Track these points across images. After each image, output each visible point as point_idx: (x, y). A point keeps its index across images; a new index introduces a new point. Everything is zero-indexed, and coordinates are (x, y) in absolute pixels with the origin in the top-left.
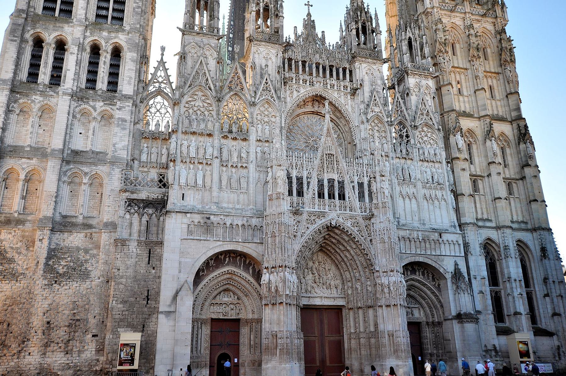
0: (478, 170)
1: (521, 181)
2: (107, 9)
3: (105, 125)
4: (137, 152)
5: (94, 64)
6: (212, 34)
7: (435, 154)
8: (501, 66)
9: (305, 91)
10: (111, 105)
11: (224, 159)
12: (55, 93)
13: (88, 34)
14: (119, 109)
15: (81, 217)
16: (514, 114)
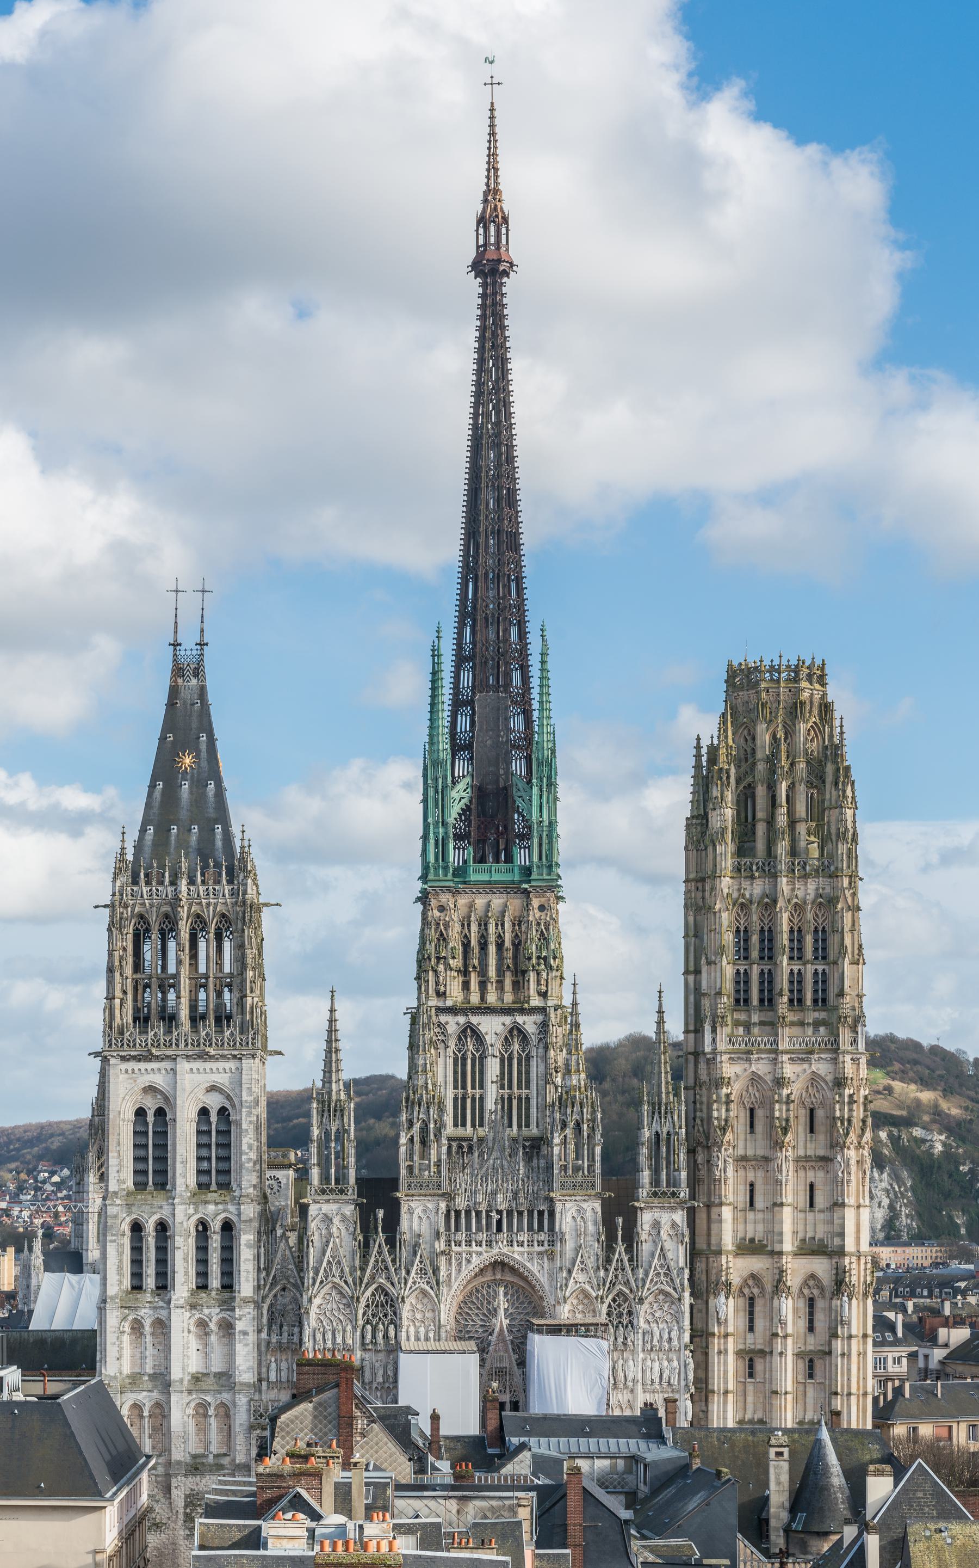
0: (760, 1341)
1: (828, 1357)
2: (209, 1159)
3: (224, 1337)
4: (264, 1370)
5: (202, 1248)
6: (343, 1197)
7: (670, 1339)
8: (832, 1147)
9: (480, 1256)
10: (228, 1310)
11: (367, 1381)
12: (165, 1302)
13: (191, 1211)
14: (240, 1319)
15: (211, 1456)
16: (837, 1241)
